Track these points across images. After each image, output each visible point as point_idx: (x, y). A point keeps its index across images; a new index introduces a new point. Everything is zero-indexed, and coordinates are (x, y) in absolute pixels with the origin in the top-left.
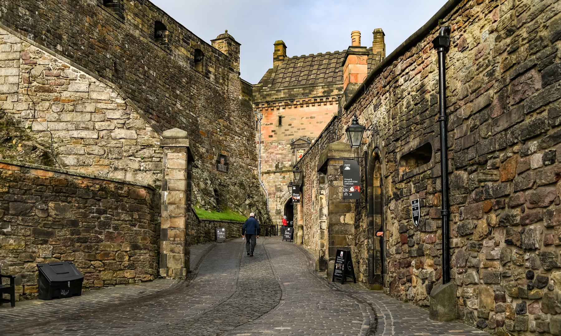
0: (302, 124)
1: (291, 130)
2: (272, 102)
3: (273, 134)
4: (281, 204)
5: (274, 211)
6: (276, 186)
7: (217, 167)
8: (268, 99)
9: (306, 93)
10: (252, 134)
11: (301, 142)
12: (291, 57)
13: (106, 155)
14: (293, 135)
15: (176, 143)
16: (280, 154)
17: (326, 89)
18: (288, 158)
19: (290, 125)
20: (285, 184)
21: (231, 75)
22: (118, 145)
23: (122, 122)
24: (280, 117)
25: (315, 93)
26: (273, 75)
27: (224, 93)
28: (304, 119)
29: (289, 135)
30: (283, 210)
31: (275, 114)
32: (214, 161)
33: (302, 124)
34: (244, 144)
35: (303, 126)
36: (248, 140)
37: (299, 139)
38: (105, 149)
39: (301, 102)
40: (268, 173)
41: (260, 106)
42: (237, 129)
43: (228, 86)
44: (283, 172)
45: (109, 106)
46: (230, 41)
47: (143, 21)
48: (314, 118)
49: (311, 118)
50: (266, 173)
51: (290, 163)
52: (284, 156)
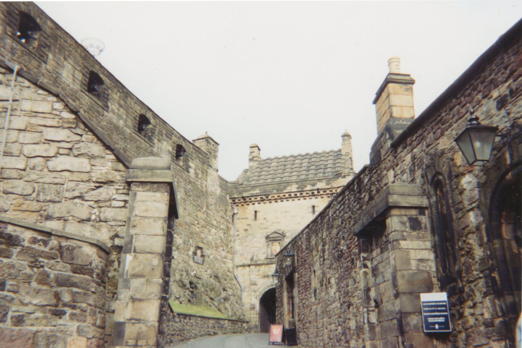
0: (277, 218)
2: (248, 197)
4: (256, 298)
7: (193, 259)
8: (245, 195)
10: (228, 227)
12: (265, 158)
13: (34, 195)
15: (152, 176)
20: (260, 277)
22: (56, 181)
23: (69, 146)
24: (256, 212)
26: (249, 173)
27: (203, 188)
29: (265, 228)
31: (251, 208)
32: (191, 253)
33: (277, 218)
34: (220, 237)
36: (224, 233)
37: (275, 232)
38: (36, 185)
40: (243, 266)
41: (237, 201)
42: (215, 223)
45: (49, 122)
46: (210, 141)
47: (127, 112)
49: (286, 212)
50: (241, 266)
51: (265, 256)
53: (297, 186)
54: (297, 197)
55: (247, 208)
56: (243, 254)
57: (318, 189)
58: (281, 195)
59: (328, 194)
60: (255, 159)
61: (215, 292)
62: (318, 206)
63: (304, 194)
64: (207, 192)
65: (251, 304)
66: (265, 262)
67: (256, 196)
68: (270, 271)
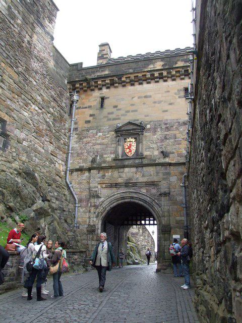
0: (132, 105)
2: (93, 79)
3: (91, 119)
4: (97, 217)
8: (89, 77)
10: (62, 116)
11: (131, 127)
12: (116, 57)
14: (119, 119)
18: (109, 149)
20: (104, 186)
21: (38, 29)
24: (103, 99)
28: (135, 99)
29: (114, 119)
30: (99, 225)
31: (97, 94)
33: (132, 105)
35: (134, 108)
37: (130, 123)
39: (132, 77)
40: (81, 170)
41: (78, 85)
43: (31, 37)
48: (150, 97)
49: (146, 97)
50: (77, 170)
51: (113, 156)
53: (162, 63)
54: (162, 78)
55: (92, 95)
58: (140, 75)
60: (105, 56)
61: (22, 198)
64: (30, 52)
65: (89, 225)
67: (104, 78)
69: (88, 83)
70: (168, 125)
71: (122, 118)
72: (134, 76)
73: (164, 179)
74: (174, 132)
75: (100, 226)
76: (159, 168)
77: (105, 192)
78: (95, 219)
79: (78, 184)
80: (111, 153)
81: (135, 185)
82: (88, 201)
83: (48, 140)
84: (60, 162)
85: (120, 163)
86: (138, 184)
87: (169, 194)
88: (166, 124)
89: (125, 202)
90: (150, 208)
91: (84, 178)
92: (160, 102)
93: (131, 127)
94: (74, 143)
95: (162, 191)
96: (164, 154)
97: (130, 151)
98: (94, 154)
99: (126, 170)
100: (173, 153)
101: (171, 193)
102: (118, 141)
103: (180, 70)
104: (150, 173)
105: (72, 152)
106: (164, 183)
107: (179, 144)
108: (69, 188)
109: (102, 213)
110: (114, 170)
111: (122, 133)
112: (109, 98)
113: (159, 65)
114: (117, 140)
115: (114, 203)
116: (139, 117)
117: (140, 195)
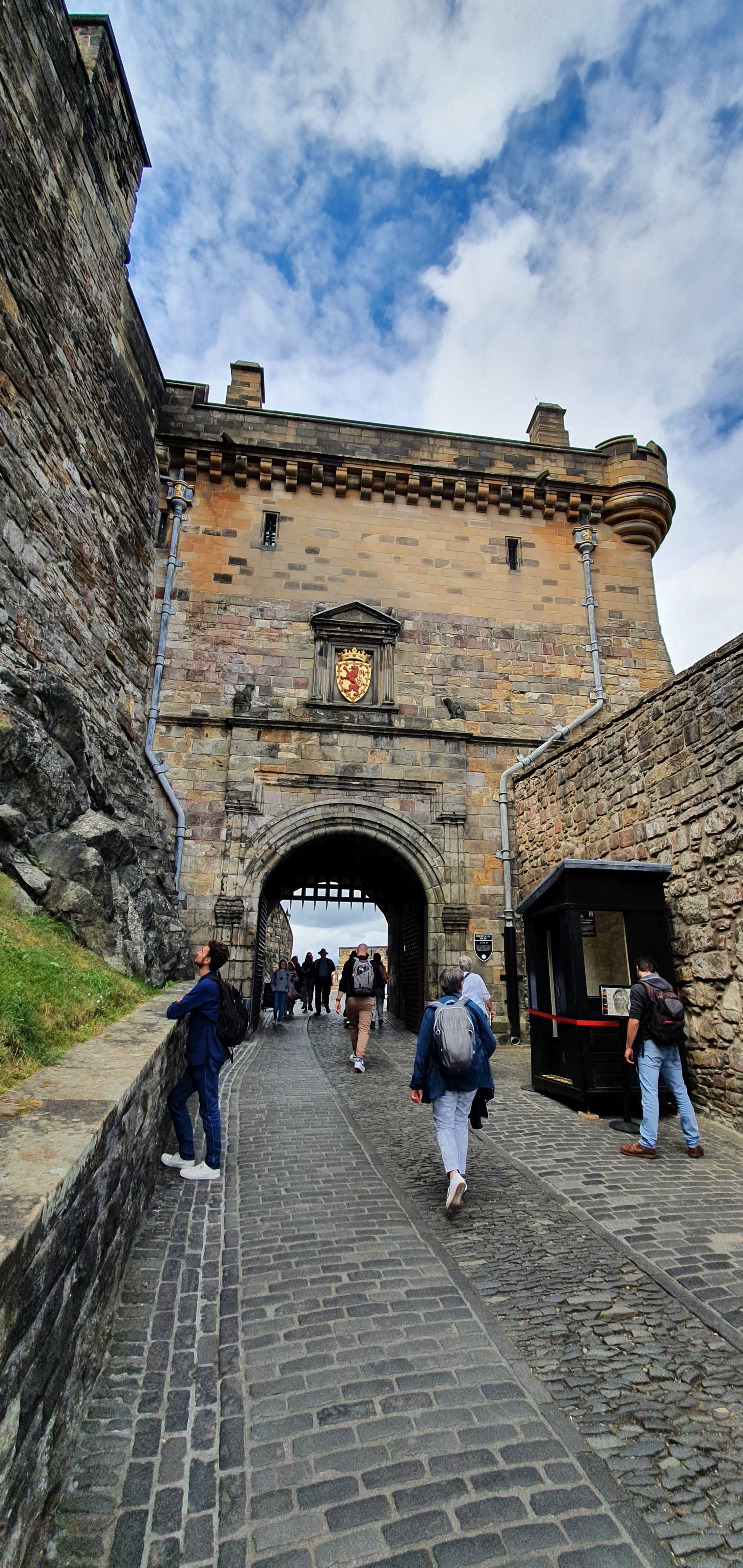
1: (313, 570)
3: (233, 570)
4: (249, 872)
5: (208, 906)
6: (227, 785)
9: (390, 450)
11: (361, 618)
14: (323, 588)
16: (258, 652)
17: (466, 453)
19: (312, 551)
24: (271, 520)
25: (426, 456)
29: (306, 587)
34: (103, 540)
35: (367, 565)
40: (197, 722)
44: (271, 726)
48: (415, 543)
50: (183, 722)
51: (304, 694)
52: (275, 662)
56: (201, 673)
57: (543, 481)
58: (391, 473)
59: (574, 507)
61: (36, 791)
62: (532, 545)
63: (484, 489)
66: (307, 720)
67: (281, 455)
68: (325, 758)
69: (228, 459)
70: (461, 632)
71: (332, 586)
72: (375, 473)
73: (452, 777)
74: (479, 653)
75: (255, 903)
76: (437, 745)
77: (275, 801)
78: (241, 880)
79: (184, 769)
80: (297, 685)
81: (368, 784)
82: (220, 822)
83: (104, 602)
84: (130, 687)
85: (328, 717)
86: (375, 782)
87: (464, 820)
88: (456, 627)
89: (337, 834)
90: (409, 856)
91: (207, 750)
92: (441, 564)
93: (361, 618)
94: (176, 636)
95: (448, 810)
96: (454, 709)
97: (356, 688)
98: (241, 678)
99: (345, 739)
100: (475, 709)
101: (470, 819)
102: (321, 653)
103: (504, 484)
104: (413, 758)
105: (167, 662)
106: (453, 789)
107: (490, 688)
108: (156, 777)
109: (265, 863)
110: (306, 735)
111: (333, 629)
112: (291, 519)
113: (445, 457)
114: (318, 649)
115: (301, 833)
116: (384, 599)
117: (382, 816)
